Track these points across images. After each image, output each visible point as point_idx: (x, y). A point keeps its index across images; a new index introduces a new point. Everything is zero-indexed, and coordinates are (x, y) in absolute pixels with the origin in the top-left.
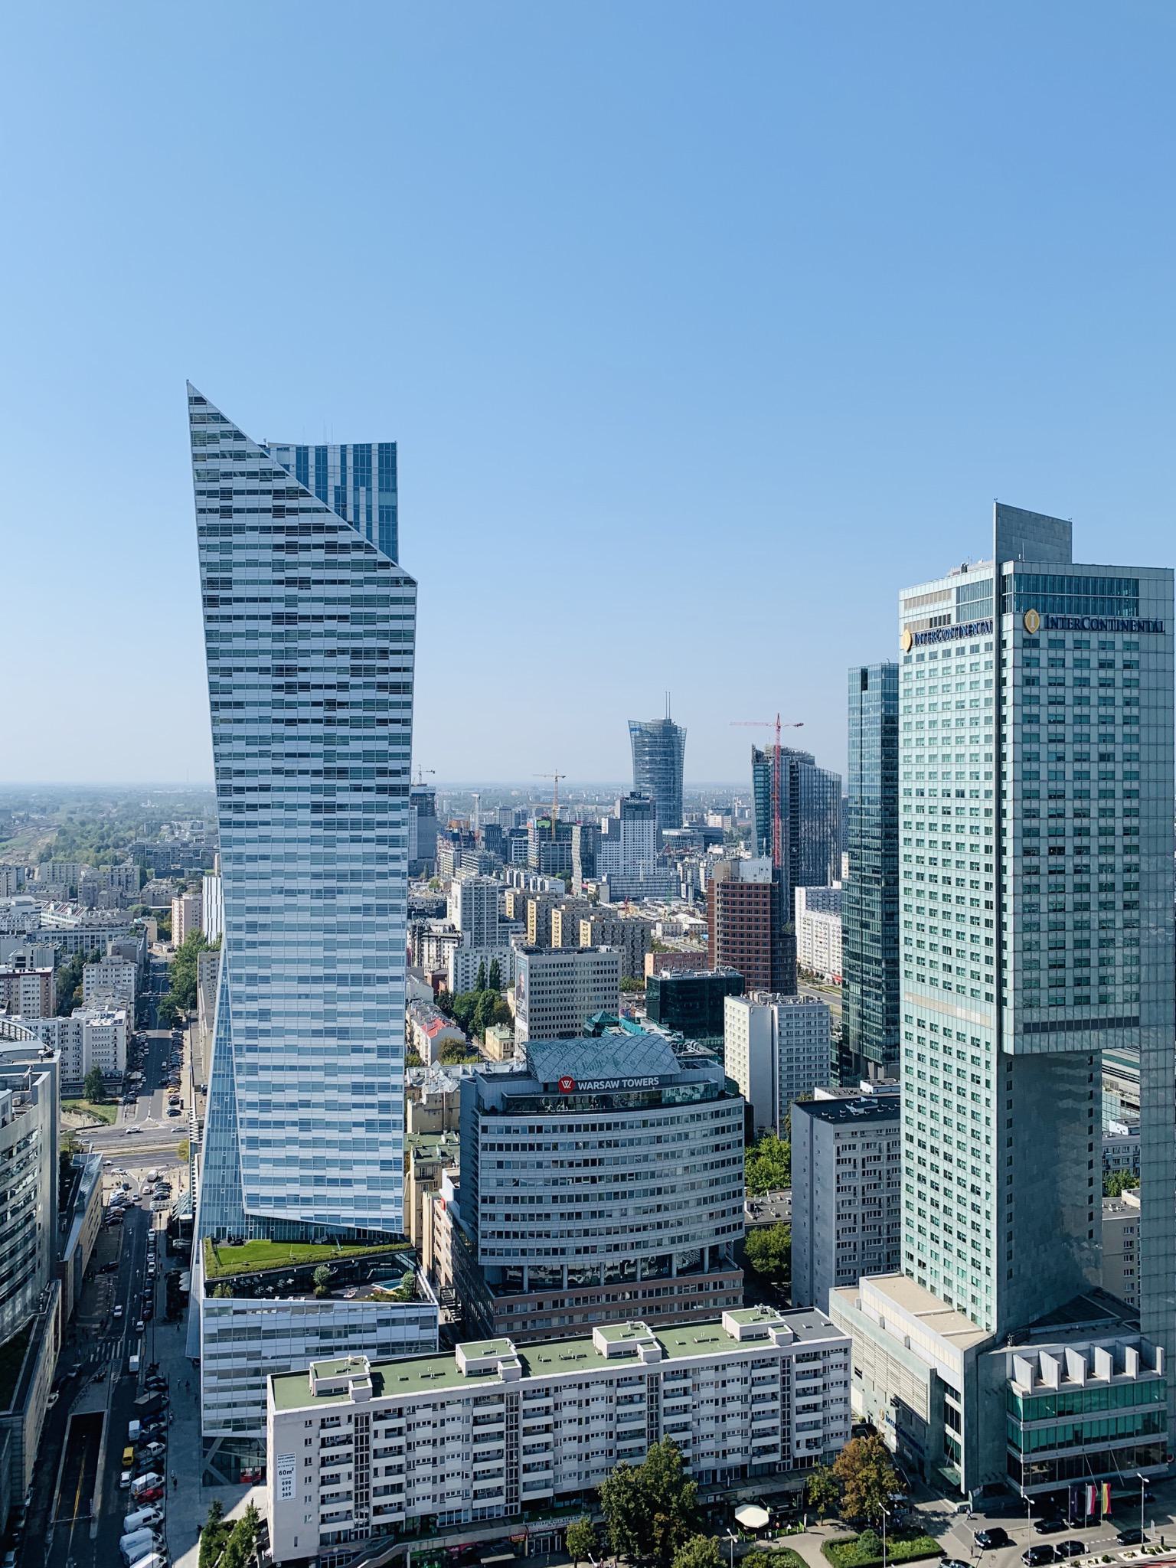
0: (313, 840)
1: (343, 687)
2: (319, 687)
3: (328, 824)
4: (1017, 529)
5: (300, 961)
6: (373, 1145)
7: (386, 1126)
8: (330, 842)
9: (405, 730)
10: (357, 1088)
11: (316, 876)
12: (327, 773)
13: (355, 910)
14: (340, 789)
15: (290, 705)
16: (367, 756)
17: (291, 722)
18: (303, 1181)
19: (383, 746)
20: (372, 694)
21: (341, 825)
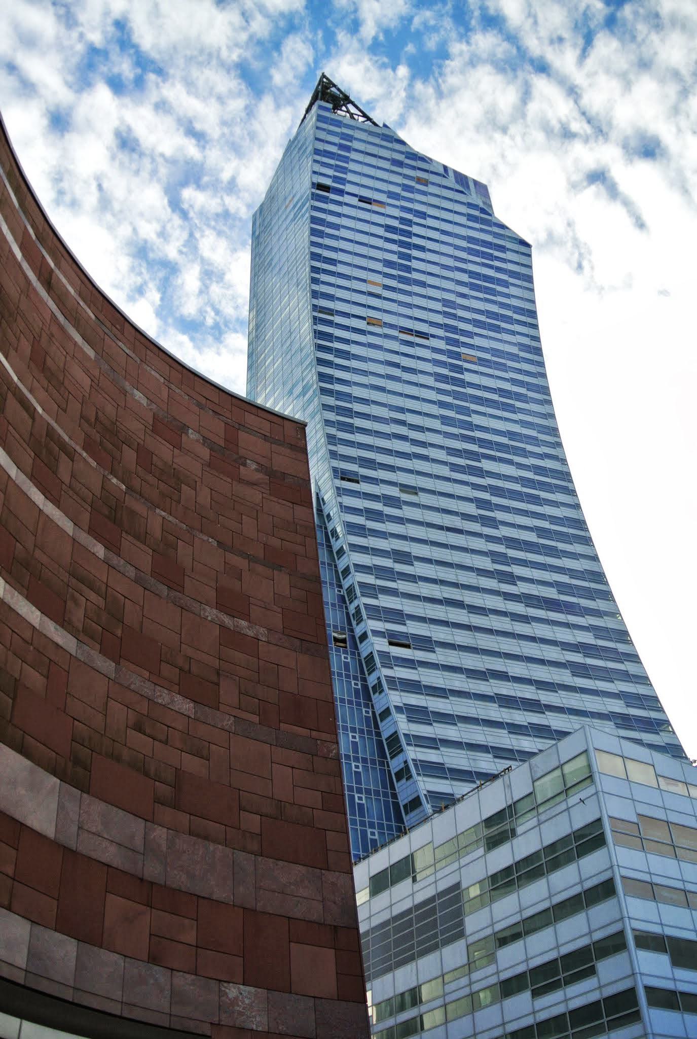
0: (442, 404)
1: (463, 296)
3: (456, 395)
11: (447, 435)
20: (494, 308)
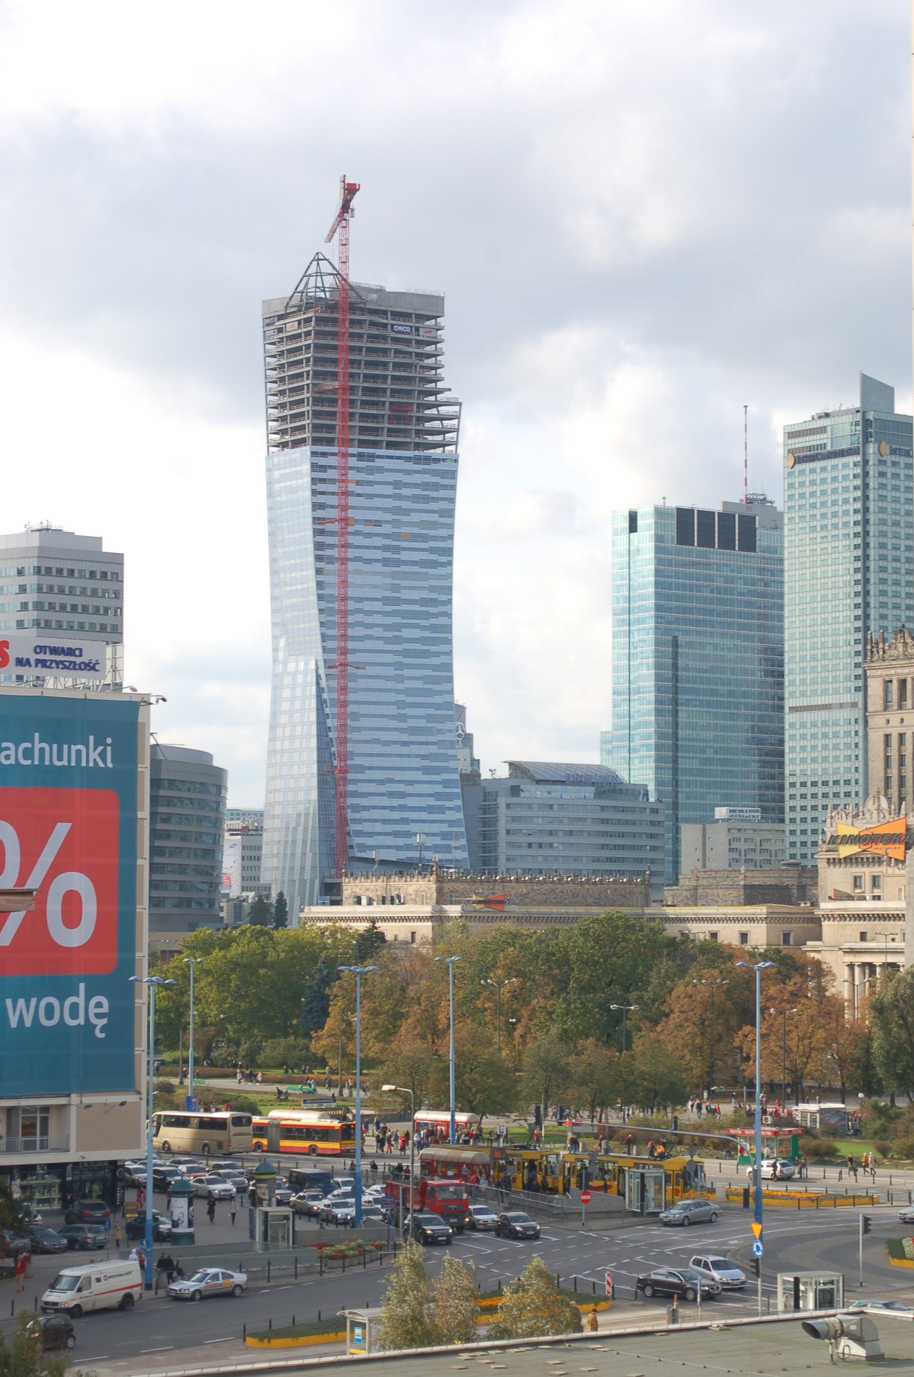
1: (407, 472)
2: (391, 470)
3: (395, 575)
5: (379, 677)
6: (442, 810)
7: (450, 797)
9: (450, 506)
10: (426, 770)
11: (386, 614)
14: (404, 549)
15: (370, 483)
16: (422, 524)
17: (370, 496)
18: (396, 834)
19: (435, 517)
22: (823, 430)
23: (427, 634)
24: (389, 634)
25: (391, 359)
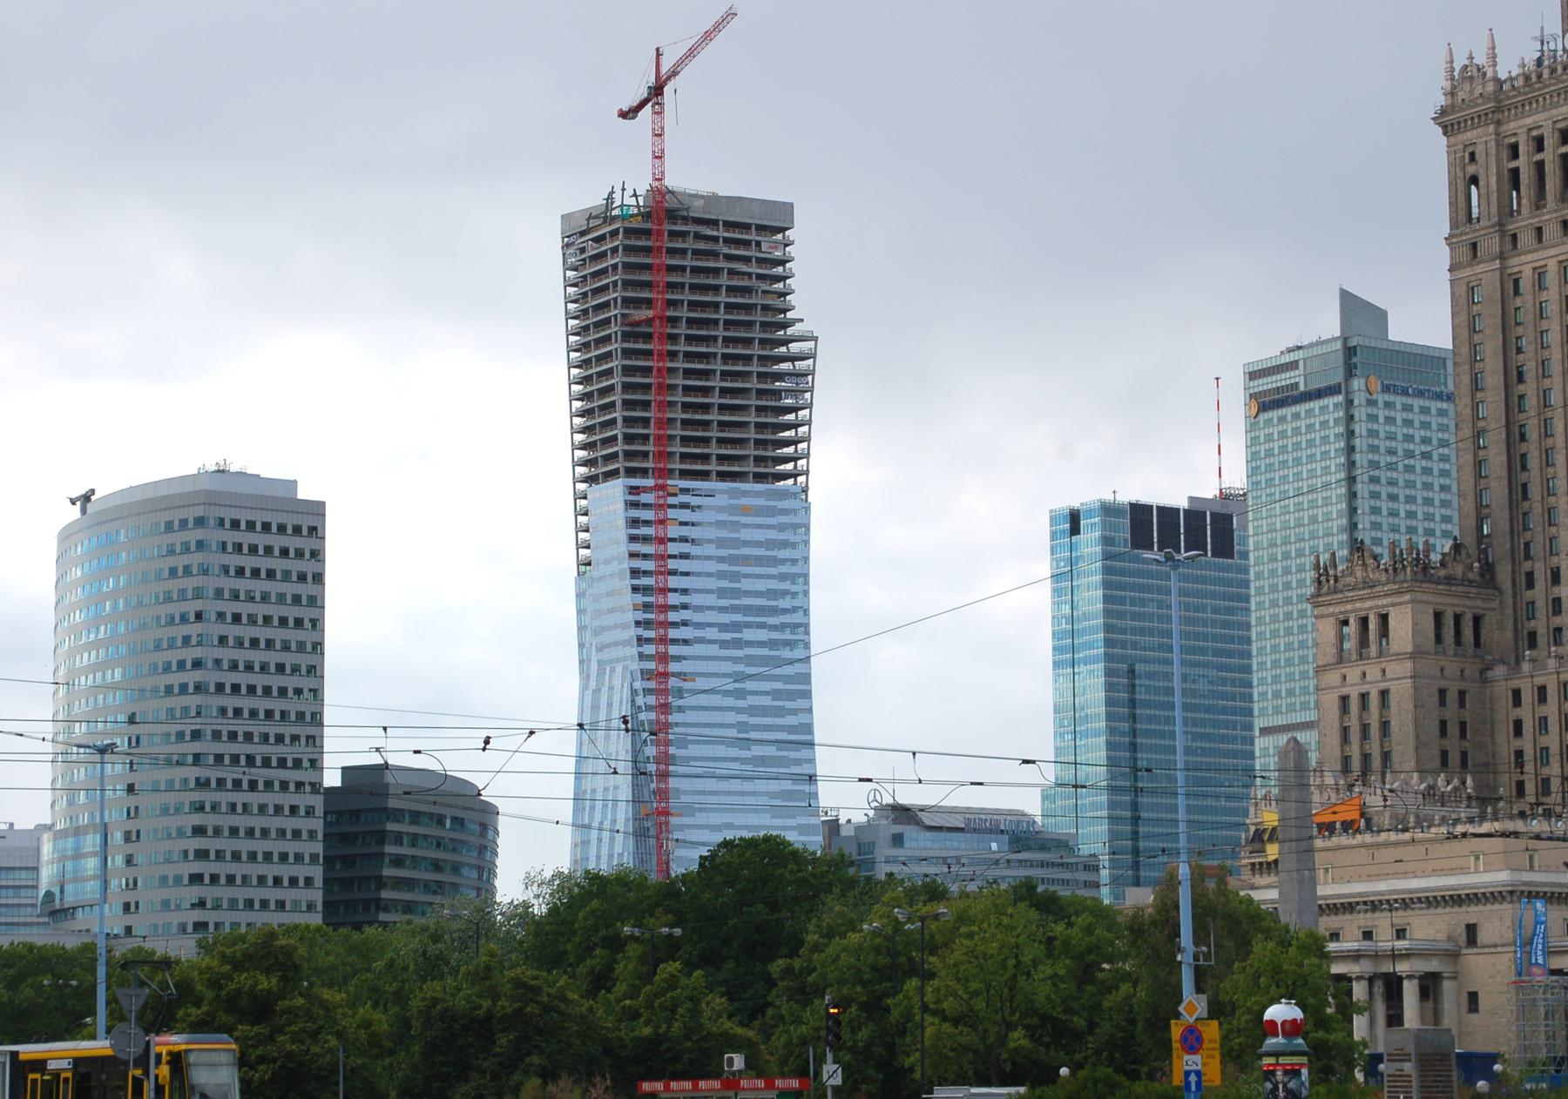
0: (721, 575)
3: (732, 560)
4: (1351, 304)
8: (736, 577)
11: (722, 610)
12: (732, 510)
13: (761, 644)
21: (746, 560)
22: (1293, 365)
23: (775, 635)
24: (727, 636)
25: (724, 280)
